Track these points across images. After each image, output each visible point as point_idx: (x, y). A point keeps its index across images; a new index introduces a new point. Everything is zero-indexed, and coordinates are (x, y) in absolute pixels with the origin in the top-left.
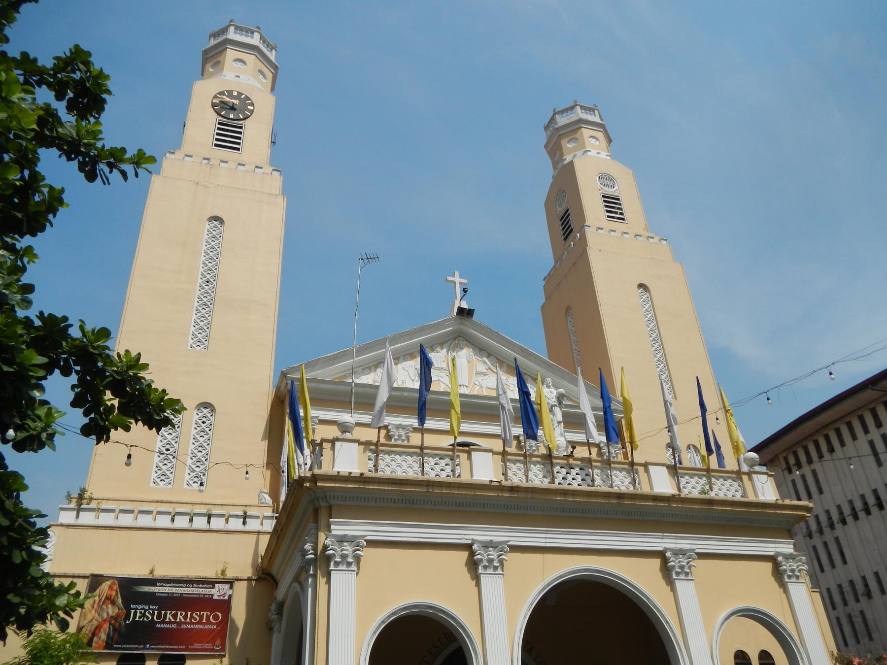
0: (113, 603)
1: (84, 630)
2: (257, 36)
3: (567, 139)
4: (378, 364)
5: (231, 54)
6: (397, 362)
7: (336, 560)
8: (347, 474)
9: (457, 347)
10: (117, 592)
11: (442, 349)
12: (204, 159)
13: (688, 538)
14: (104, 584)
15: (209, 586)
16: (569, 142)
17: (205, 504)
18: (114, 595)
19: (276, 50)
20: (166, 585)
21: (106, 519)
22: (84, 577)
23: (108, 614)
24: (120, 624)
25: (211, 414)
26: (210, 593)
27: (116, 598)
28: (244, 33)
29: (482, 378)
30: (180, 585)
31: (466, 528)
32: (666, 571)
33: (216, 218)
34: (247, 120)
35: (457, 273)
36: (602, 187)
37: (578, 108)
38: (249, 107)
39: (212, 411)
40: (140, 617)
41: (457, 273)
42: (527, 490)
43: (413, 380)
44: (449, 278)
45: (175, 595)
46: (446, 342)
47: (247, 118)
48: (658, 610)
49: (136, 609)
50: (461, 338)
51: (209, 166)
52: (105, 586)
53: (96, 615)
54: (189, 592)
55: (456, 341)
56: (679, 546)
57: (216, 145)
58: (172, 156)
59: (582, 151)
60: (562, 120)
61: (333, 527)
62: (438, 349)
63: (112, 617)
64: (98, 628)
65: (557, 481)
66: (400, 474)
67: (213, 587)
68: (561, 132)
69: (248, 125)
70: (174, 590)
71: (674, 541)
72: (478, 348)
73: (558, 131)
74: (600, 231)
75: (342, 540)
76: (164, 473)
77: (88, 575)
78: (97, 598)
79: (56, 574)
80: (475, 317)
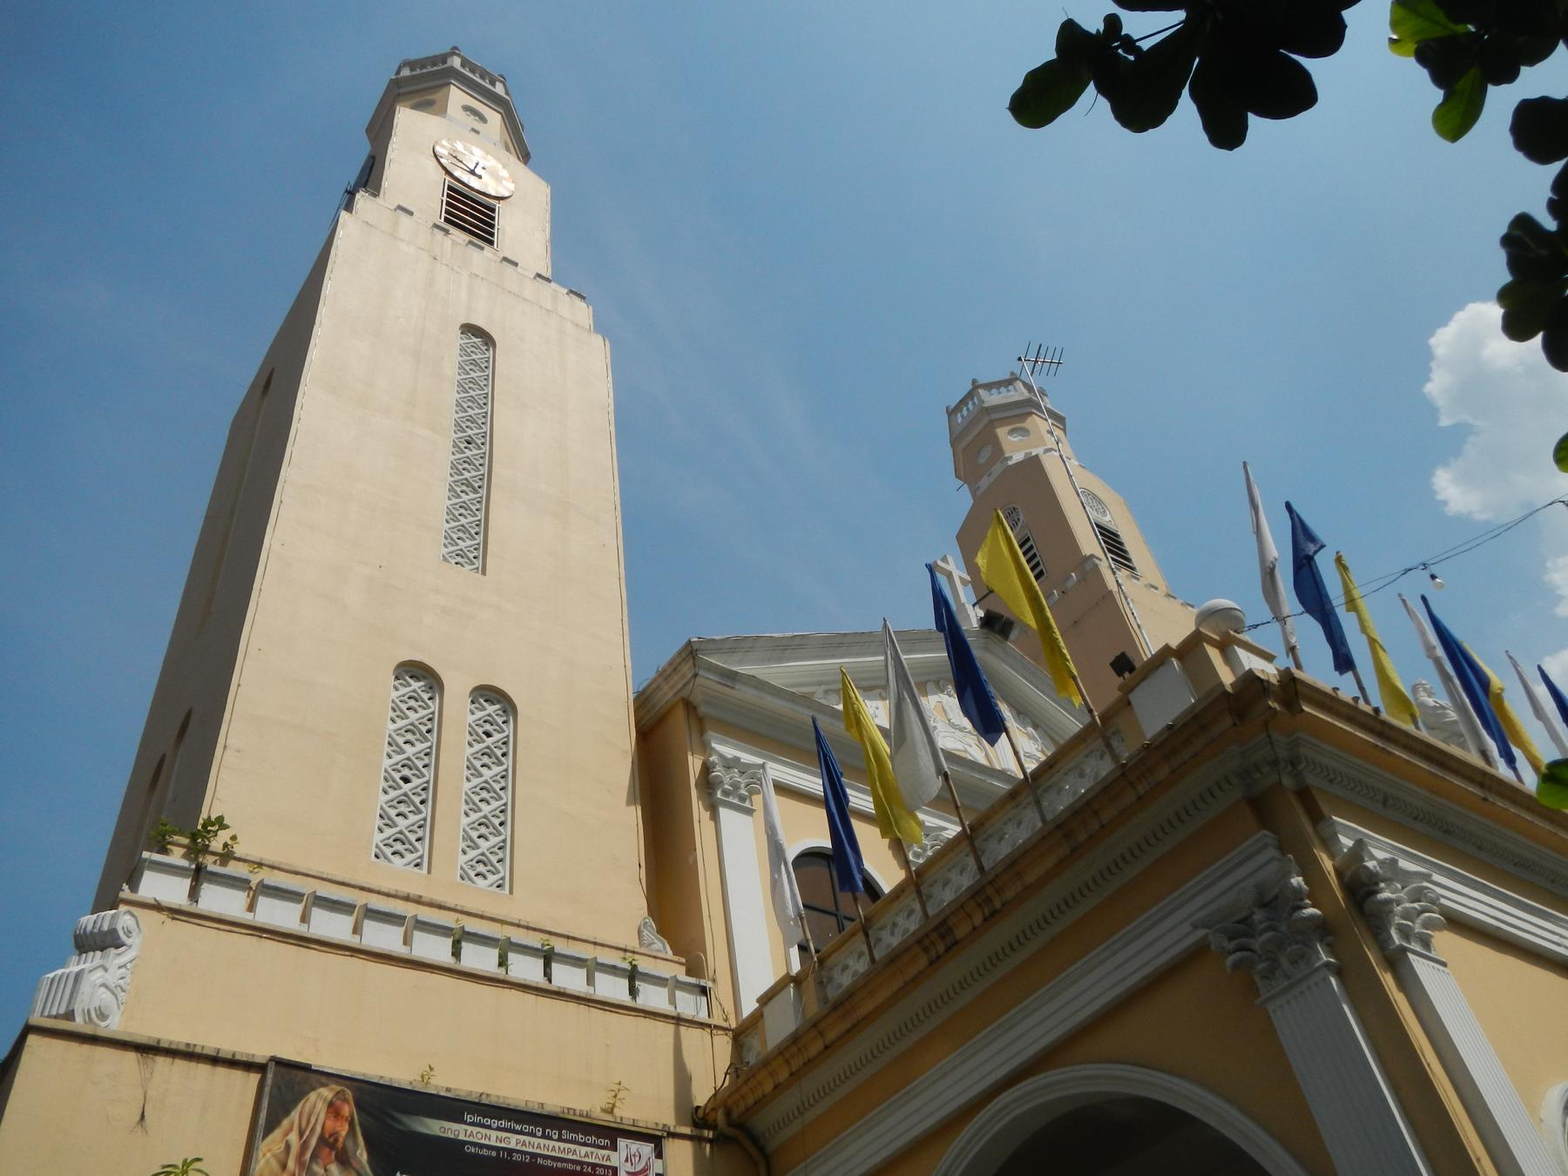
3: (1010, 427)
10: (351, 1124)
14: (313, 1096)
15: (603, 1142)
16: (1011, 432)
17: (528, 928)
18: (344, 1133)
20: (487, 1121)
22: (248, 1066)
25: (505, 718)
26: (608, 1163)
27: (350, 1144)
30: (527, 1128)
39: (504, 712)
45: (516, 1157)
52: (317, 1100)
54: (553, 1154)
67: (614, 1148)
68: (994, 416)
70: (513, 1141)
72: (1016, 709)
73: (989, 414)
76: (401, 836)
77: (260, 1060)
78: (293, 1137)
79: (163, 1045)
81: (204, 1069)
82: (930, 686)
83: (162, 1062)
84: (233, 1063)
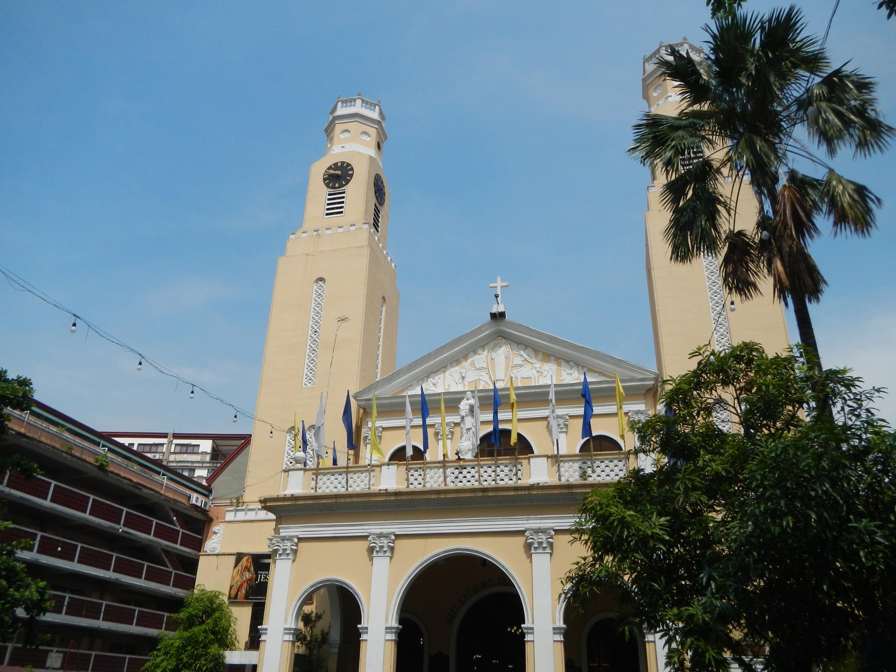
0: (249, 571)
2: (359, 102)
3: (653, 88)
4: (430, 374)
5: (339, 128)
8: (283, 496)
9: (497, 346)
13: (552, 518)
19: (379, 106)
22: (234, 555)
29: (518, 370)
32: (528, 547)
33: (321, 279)
35: (499, 279)
38: (350, 172)
41: (499, 279)
44: (492, 285)
46: (486, 345)
48: (514, 578)
49: (261, 574)
50: (500, 338)
51: (317, 236)
52: (245, 559)
55: (496, 341)
56: (538, 525)
57: (327, 214)
59: (663, 99)
61: (281, 531)
62: (480, 352)
65: (449, 480)
71: (539, 521)
75: (284, 539)
78: (240, 568)
80: (508, 317)
81: (227, 556)
82: (462, 359)
83: (220, 556)
84: (231, 555)
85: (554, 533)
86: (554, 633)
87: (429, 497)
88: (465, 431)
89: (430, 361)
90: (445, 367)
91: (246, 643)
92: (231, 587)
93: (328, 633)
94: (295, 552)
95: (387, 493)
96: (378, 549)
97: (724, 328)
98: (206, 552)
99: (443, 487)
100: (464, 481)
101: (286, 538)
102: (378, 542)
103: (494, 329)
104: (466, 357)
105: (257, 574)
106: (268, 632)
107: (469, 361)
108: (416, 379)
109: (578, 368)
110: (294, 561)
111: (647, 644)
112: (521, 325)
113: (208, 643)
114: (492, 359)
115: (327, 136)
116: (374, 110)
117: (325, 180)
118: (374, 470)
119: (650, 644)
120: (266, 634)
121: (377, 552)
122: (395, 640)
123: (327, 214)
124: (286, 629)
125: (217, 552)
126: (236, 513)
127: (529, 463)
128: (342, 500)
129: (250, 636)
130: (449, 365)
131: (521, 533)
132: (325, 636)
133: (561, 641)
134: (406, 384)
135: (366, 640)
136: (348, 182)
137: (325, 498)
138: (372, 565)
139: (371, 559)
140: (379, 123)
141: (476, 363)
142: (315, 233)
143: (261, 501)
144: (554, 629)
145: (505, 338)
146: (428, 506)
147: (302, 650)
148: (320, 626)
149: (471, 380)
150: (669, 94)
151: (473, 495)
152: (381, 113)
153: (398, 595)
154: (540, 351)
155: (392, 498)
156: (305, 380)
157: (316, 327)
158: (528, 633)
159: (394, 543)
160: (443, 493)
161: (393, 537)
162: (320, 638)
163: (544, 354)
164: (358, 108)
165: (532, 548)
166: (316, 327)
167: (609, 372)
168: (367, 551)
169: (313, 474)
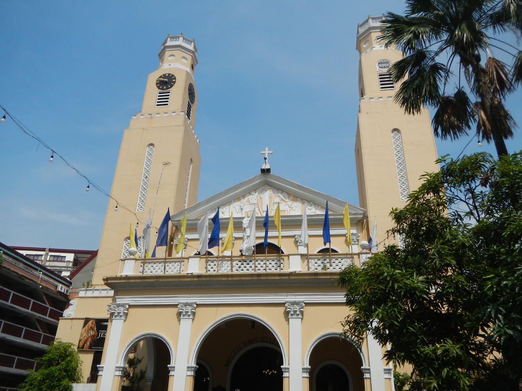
0: (93, 330)
1: (81, 341)
3: (364, 42)
5: (168, 53)
6: (230, 204)
7: (115, 315)
8: (120, 276)
9: (264, 190)
11: (255, 193)
12: (149, 115)
16: (364, 44)
19: (194, 42)
21: (97, 294)
22: (83, 319)
23: (91, 334)
24: (95, 338)
28: (175, 39)
31: (177, 297)
32: (287, 314)
33: (152, 145)
34: (172, 88)
35: (267, 149)
36: (380, 69)
37: (370, 20)
38: (173, 80)
40: (103, 336)
41: (267, 149)
42: (206, 276)
43: (238, 212)
44: (262, 152)
46: (258, 189)
47: (172, 86)
48: (276, 335)
49: (101, 332)
50: (266, 185)
52: (90, 322)
53: (86, 335)
55: (264, 187)
56: (294, 300)
57: (157, 105)
58: (135, 117)
59: (370, 49)
60: (361, 30)
61: (117, 300)
62: (253, 193)
63: (92, 336)
64: (86, 340)
65: (234, 269)
66: (155, 273)
69: (173, 90)
71: (294, 297)
72: (276, 188)
74: (371, 100)
75: (119, 305)
78: (87, 328)
81: (78, 320)
82: (241, 198)
83: (73, 320)
84: (82, 319)
85: (304, 305)
86: (303, 372)
87: (221, 279)
88: (245, 237)
89: (221, 198)
90: (231, 202)
91: (88, 378)
92: (80, 341)
93: (145, 372)
94: (126, 315)
95: (192, 276)
96: (184, 314)
97: (405, 185)
98: (64, 317)
99: (230, 273)
100: (245, 269)
101: (121, 305)
102: (184, 309)
103: (262, 179)
104: (244, 197)
105: (98, 332)
106: (104, 369)
107: (246, 199)
108: (211, 209)
109: (315, 205)
110: (125, 321)
111: (365, 380)
112: (281, 178)
113: (61, 378)
114: (261, 198)
115: (160, 58)
116: (191, 45)
117: (157, 84)
118: (184, 261)
119: (367, 379)
120: (102, 370)
121: (184, 315)
122: (193, 376)
123: (157, 105)
124: (117, 367)
125: (71, 317)
126: (86, 292)
127: (289, 259)
128: (161, 280)
129: (91, 374)
130: (233, 201)
131: (282, 304)
132: (143, 374)
133: (307, 377)
134: (203, 212)
135: (173, 376)
136: (172, 86)
137: (149, 278)
138: (180, 324)
139: (179, 320)
140: (193, 52)
141: (250, 200)
142: (149, 116)
143: (104, 280)
144: (303, 369)
145: (269, 186)
146: (220, 285)
147: (126, 383)
148: (140, 367)
149: (247, 211)
150: (373, 46)
151: (251, 278)
152: (195, 47)
153: (197, 345)
154: (291, 194)
155: (196, 279)
156: (137, 208)
157: (147, 174)
158: (285, 372)
159: (195, 310)
160: (230, 277)
161: (195, 306)
162: (139, 375)
163: (294, 196)
164: (180, 42)
165: (290, 315)
166: (147, 174)
167: (333, 209)
168: (176, 315)
169: (142, 262)
